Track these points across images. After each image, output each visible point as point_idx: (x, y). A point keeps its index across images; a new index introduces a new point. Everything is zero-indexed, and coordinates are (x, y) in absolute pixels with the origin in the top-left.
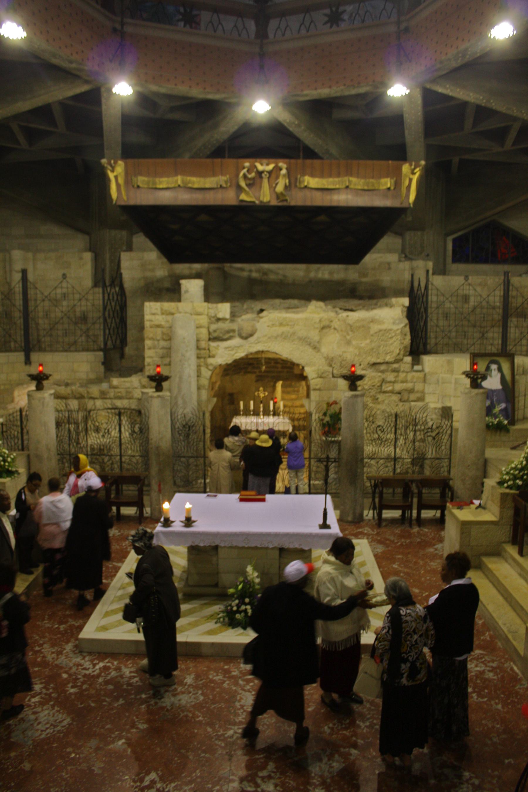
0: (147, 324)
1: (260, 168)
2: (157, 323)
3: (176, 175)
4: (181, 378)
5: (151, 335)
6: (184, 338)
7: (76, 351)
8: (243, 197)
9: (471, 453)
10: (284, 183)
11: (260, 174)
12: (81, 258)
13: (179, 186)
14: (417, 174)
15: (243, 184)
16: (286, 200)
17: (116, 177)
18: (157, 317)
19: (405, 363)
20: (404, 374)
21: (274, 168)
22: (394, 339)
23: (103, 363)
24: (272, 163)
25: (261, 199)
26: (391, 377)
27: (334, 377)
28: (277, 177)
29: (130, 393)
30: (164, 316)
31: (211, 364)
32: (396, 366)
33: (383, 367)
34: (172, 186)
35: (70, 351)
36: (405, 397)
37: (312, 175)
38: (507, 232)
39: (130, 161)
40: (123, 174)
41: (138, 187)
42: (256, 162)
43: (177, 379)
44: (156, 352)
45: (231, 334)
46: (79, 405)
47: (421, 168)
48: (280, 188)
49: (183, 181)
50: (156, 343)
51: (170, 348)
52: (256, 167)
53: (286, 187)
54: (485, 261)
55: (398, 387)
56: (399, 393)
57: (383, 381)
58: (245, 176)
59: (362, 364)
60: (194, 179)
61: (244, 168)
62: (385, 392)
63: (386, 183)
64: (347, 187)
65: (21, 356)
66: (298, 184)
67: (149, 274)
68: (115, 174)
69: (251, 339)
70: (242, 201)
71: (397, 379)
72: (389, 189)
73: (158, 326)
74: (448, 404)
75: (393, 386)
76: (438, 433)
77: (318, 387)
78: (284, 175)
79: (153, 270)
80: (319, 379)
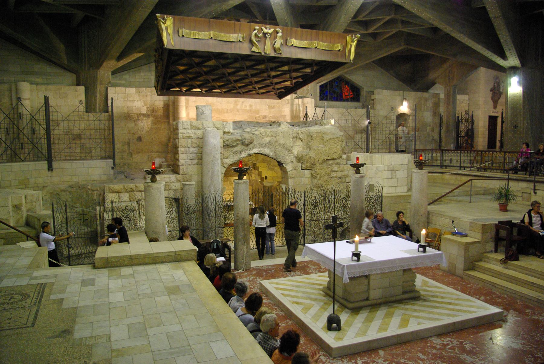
0: (180, 136)
1: (265, 31)
2: (188, 135)
3: (209, 30)
4: (213, 173)
5: (184, 144)
6: (215, 145)
7: (91, 159)
8: (254, 49)
9: (422, 207)
10: (280, 42)
11: (265, 34)
12: (76, 91)
13: (212, 38)
14: (355, 42)
15: (254, 40)
16: (281, 53)
17: (166, 28)
18: (188, 131)
19: (343, 159)
20: (343, 166)
21: (273, 31)
22: (337, 144)
23: (113, 168)
24: (272, 28)
25: (265, 51)
26: (335, 168)
27: (302, 169)
28: (275, 38)
29: (169, 186)
30: (193, 130)
31: (226, 163)
32: (337, 161)
33: (331, 162)
34: (207, 38)
35: (87, 159)
36: (344, 180)
37: (296, 39)
38: (348, 82)
39: (176, 17)
40: (171, 26)
41: (183, 36)
42: (262, 26)
43: (210, 174)
44: (188, 156)
45: (238, 143)
46: (130, 196)
47: (357, 38)
48: (277, 45)
49: (214, 36)
50: (187, 149)
51: (202, 153)
52: (262, 30)
53: (282, 45)
54: (337, 100)
55: (339, 174)
56: (340, 178)
57: (332, 171)
58: (256, 35)
59: (320, 160)
60: (223, 34)
61: (255, 30)
62: (331, 178)
63: (338, 47)
64: (316, 47)
65: (45, 164)
66: (287, 44)
67: (130, 104)
68: (166, 25)
69: (251, 146)
70: (253, 52)
71: (339, 169)
72: (339, 50)
73: (189, 137)
74: (371, 183)
75: (337, 173)
76: (375, 200)
77: (293, 176)
78: (281, 37)
79: (133, 101)
80: (294, 171)
